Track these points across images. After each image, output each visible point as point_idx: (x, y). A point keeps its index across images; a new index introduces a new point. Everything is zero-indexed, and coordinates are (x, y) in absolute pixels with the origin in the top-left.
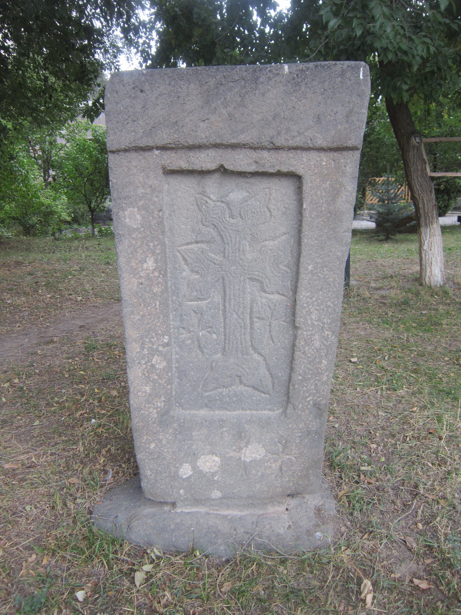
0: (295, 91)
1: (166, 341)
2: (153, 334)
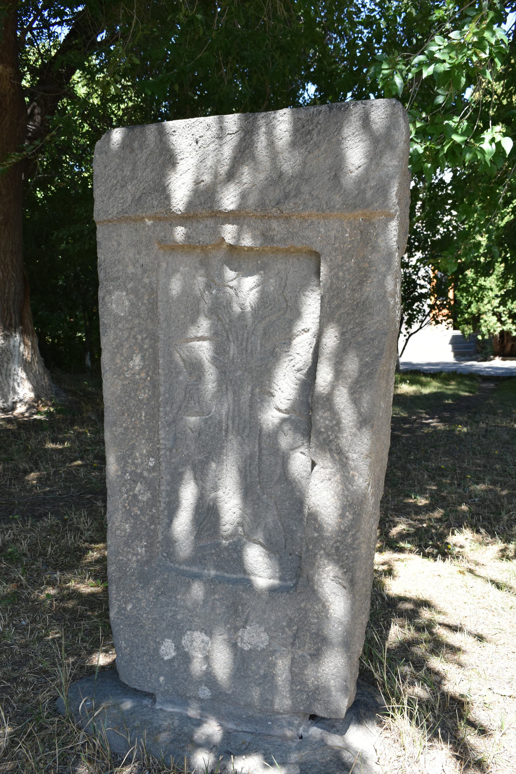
1: (151, 464)
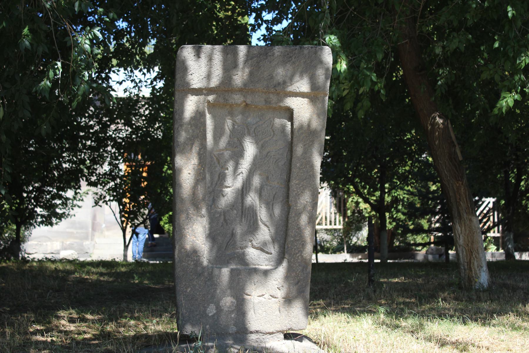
0: (289, 61)
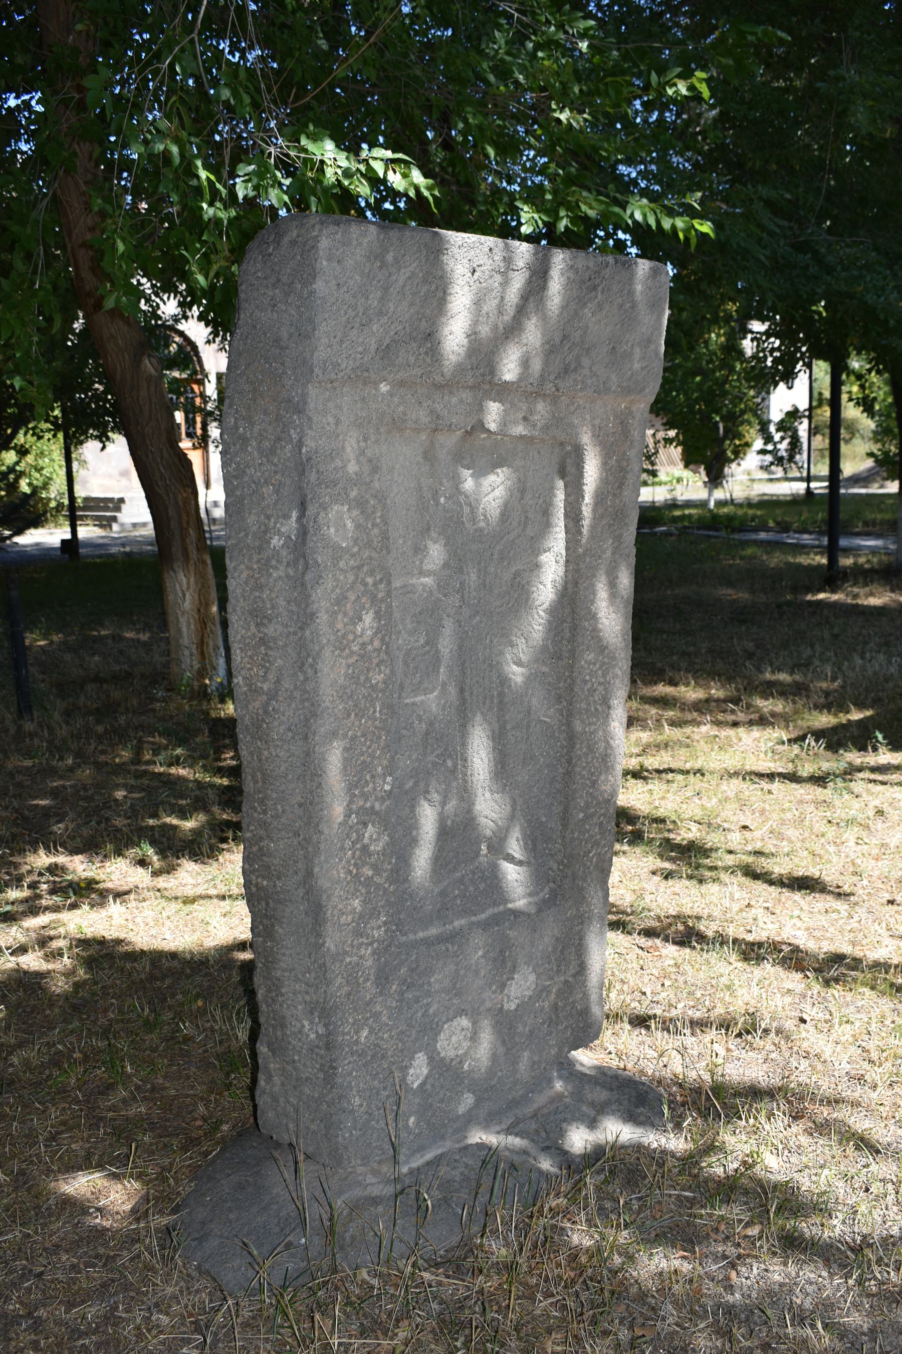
1: (387, 787)
2: (368, 778)
